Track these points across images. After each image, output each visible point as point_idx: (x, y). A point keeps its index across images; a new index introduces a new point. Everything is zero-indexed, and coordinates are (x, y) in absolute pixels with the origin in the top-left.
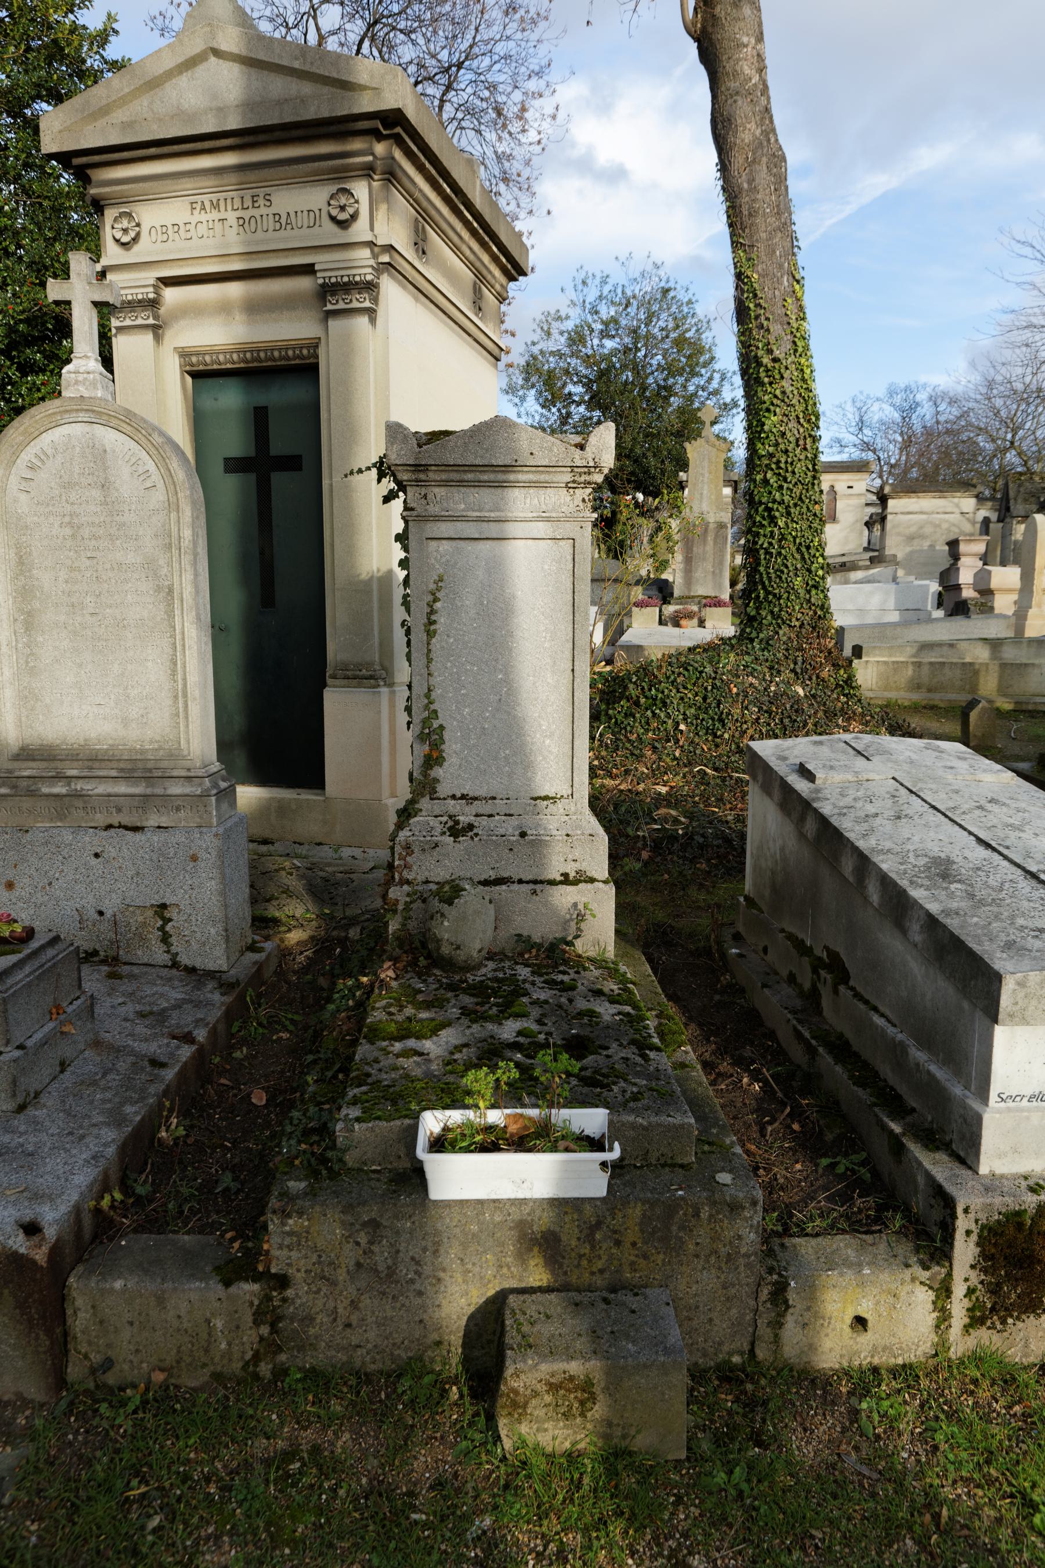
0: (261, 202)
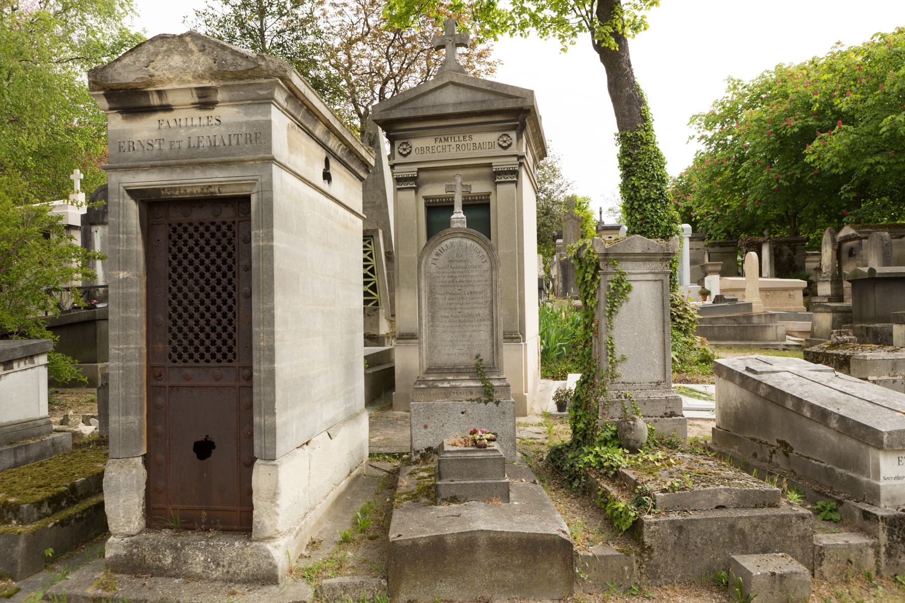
0: (467, 138)
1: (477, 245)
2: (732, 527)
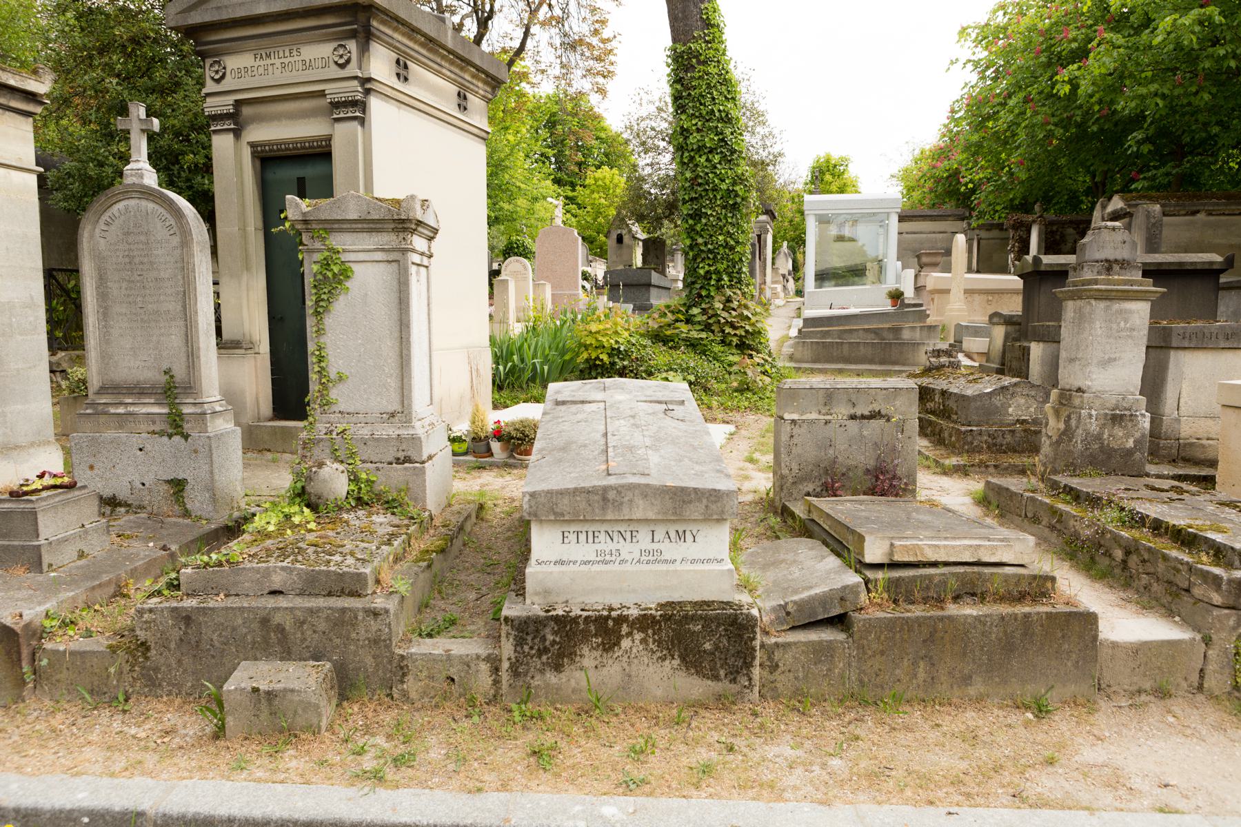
0: (295, 53)
1: (161, 210)
2: (265, 621)
